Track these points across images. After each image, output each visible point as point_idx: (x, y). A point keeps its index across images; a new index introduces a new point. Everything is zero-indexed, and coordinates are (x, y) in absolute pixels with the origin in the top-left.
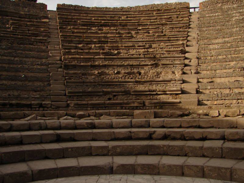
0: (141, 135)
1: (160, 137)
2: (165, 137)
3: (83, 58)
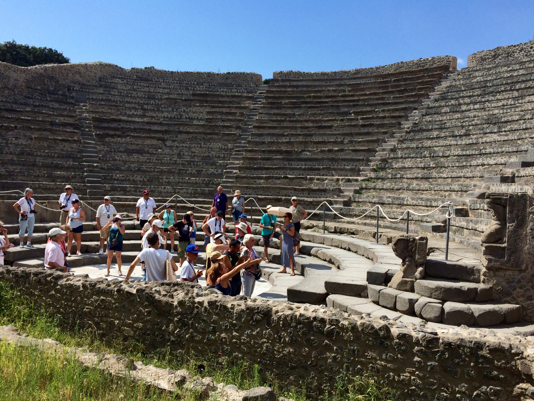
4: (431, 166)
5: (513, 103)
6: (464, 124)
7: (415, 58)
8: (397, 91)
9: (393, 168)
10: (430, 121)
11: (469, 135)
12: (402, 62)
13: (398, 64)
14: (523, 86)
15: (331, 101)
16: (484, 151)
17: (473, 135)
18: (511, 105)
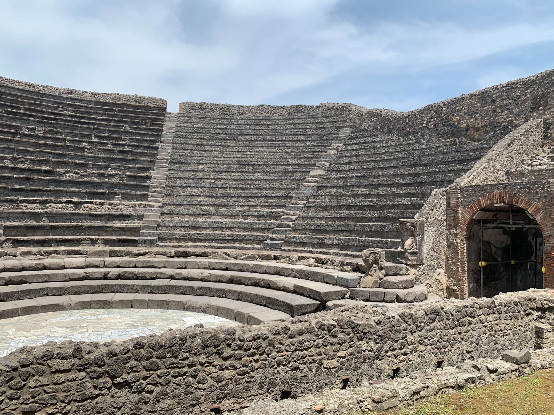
0: (96, 276)
1: (114, 277)
2: (119, 277)
3: (17, 178)
4: (219, 195)
5: (245, 150)
6: (219, 162)
7: (132, 94)
8: (131, 121)
9: (181, 196)
10: (182, 155)
11: (229, 172)
12: (118, 94)
13: (115, 94)
14: (243, 138)
15: (61, 119)
16: (258, 186)
17: (232, 172)
18: (244, 152)
